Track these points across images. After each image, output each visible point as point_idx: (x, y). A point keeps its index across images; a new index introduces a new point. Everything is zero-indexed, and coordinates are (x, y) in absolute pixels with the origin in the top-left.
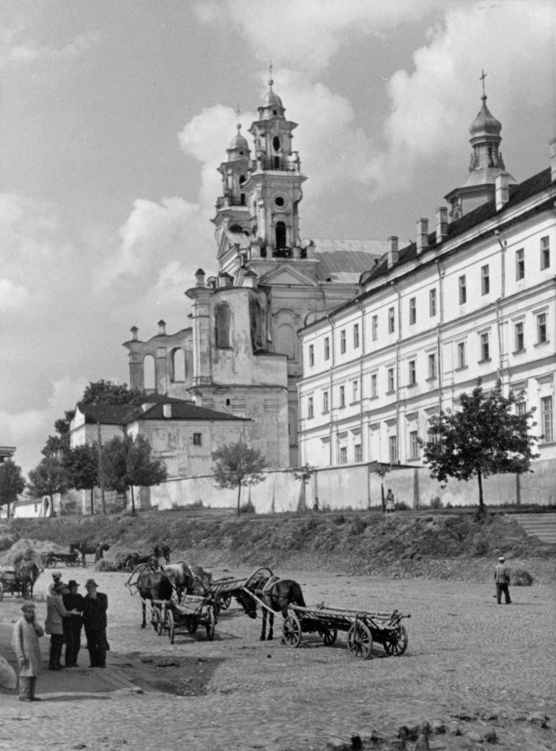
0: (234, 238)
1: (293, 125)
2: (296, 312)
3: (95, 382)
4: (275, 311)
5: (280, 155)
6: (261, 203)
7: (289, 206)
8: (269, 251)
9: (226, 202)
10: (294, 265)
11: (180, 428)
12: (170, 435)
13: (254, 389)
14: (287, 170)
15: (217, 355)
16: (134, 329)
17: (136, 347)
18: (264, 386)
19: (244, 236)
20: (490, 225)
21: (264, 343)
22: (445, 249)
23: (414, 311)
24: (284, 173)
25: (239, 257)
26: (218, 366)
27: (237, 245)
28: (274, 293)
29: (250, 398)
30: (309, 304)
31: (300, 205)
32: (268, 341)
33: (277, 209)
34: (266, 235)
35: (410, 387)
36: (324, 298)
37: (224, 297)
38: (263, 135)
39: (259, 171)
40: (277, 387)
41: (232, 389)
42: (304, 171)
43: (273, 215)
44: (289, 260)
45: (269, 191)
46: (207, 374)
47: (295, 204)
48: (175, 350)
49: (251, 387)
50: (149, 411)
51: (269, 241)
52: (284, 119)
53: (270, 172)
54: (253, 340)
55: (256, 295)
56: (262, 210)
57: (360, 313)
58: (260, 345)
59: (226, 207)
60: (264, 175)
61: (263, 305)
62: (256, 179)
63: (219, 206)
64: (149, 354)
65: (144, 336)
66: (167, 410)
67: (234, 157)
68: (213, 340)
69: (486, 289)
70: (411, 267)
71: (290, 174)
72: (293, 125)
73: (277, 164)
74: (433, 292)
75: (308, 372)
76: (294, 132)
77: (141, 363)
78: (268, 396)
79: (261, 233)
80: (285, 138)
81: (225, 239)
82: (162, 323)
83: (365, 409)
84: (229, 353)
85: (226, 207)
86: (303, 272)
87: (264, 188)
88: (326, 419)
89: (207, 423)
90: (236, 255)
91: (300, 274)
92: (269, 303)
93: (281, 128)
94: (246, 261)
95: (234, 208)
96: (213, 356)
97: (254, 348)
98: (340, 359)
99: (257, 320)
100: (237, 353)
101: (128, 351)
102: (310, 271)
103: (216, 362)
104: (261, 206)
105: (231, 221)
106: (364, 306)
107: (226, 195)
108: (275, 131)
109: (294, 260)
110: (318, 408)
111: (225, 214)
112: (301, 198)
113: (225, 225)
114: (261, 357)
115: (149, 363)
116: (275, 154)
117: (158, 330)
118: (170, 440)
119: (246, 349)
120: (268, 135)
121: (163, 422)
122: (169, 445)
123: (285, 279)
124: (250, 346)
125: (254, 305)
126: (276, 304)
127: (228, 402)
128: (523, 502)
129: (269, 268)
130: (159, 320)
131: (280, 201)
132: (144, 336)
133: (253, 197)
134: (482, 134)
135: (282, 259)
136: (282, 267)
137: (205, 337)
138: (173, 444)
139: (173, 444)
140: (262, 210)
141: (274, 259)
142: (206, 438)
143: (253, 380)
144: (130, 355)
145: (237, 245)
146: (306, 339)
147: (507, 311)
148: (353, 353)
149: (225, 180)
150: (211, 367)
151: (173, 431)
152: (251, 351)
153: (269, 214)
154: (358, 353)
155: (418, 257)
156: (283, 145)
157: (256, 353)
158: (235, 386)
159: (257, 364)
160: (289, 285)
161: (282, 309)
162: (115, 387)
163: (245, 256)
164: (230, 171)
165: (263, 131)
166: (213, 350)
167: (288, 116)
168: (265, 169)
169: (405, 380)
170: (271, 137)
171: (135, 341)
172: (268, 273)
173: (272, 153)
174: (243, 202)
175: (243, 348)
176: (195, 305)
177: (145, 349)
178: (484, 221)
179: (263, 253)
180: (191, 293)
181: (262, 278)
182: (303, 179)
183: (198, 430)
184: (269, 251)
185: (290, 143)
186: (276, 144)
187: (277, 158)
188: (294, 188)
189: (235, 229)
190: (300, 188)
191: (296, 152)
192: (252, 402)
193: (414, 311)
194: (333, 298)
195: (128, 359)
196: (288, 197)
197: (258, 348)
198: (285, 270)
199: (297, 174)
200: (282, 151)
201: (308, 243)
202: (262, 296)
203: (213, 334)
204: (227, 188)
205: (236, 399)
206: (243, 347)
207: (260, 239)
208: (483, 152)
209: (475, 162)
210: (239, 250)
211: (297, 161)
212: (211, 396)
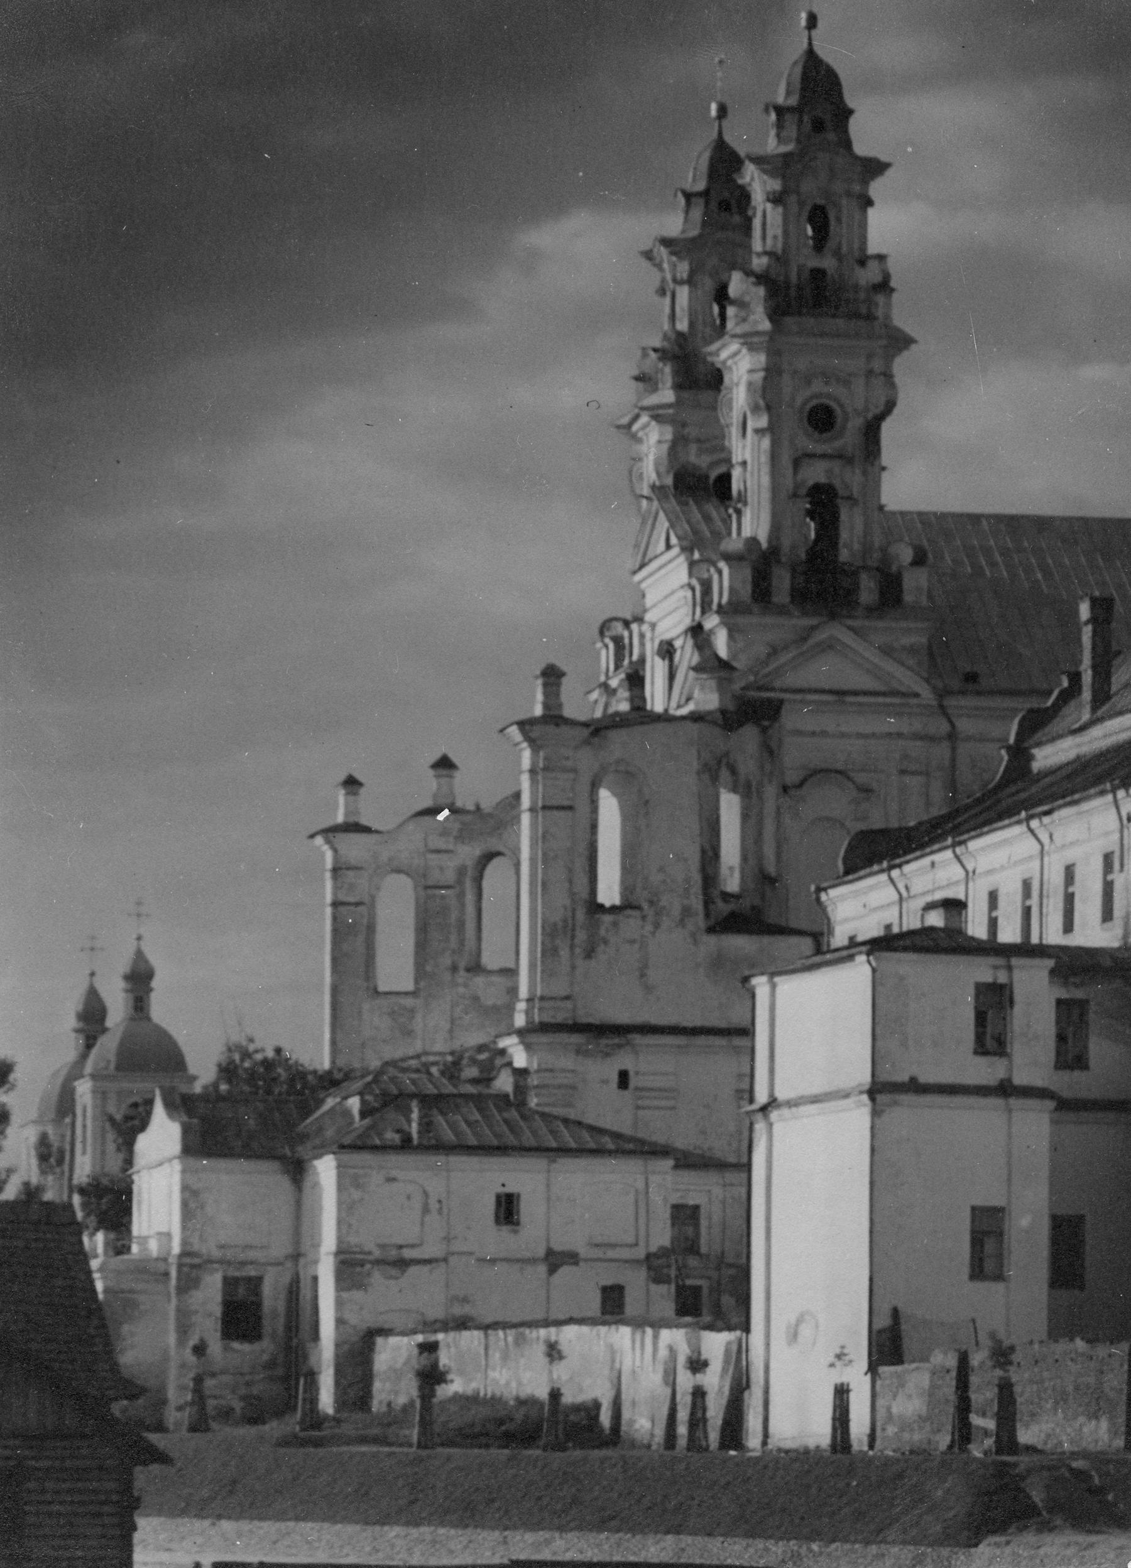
1: (875, 168)
2: (861, 778)
4: (792, 777)
5: (828, 263)
7: (850, 437)
13: (701, 1040)
17: (355, 847)
23: (1069, 899)
26: (593, 963)
28: (790, 720)
30: (905, 757)
31: (888, 429)
36: (952, 736)
38: (776, 199)
41: (637, 1039)
43: (797, 463)
45: (787, 383)
46: (560, 988)
48: (489, 857)
51: (786, 543)
52: (847, 144)
64: (399, 871)
72: (875, 168)
76: (876, 188)
77: (369, 904)
82: (444, 764)
85: (666, 395)
87: (772, 372)
91: (876, 659)
100: (657, 925)
102: (912, 650)
103: (589, 954)
107: (663, 354)
112: (890, 406)
116: (814, 263)
119: (686, 912)
120: (793, 199)
124: (697, 904)
127: (624, 1079)
130: (435, 756)
136: (821, 636)
142: (530, 1210)
150: (573, 967)
152: (701, 921)
153: (786, 460)
159: (718, 963)
161: (816, 772)
165: (776, 185)
166: (581, 915)
170: (801, 204)
171: (353, 827)
175: (676, 911)
184: (782, 582)
185: (863, 225)
187: (818, 274)
188: (870, 373)
190: (888, 376)
191: (881, 258)
197: (722, 908)
198: (829, 646)
200: (838, 254)
202: (749, 735)
206: (673, 903)
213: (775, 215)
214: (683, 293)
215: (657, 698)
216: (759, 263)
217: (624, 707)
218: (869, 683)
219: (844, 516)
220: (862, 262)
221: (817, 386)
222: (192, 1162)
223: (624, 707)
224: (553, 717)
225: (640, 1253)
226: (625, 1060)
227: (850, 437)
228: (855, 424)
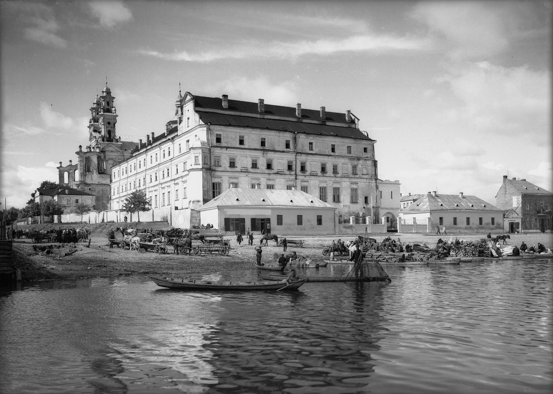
0: (94, 134)
1: (114, 98)
2: (114, 160)
3: (44, 181)
4: (107, 159)
5: (109, 108)
6: (103, 123)
7: (112, 125)
8: (105, 139)
9: (93, 122)
10: (113, 144)
11: (71, 198)
12: (68, 200)
14: (112, 113)
15: (86, 174)
16: (61, 163)
18: (102, 184)
19: (98, 133)
20: (164, 140)
21: (103, 170)
22: (148, 148)
23: (140, 164)
24: (110, 114)
25: (95, 141)
27: (95, 137)
28: (107, 153)
29: (97, 188)
32: (104, 169)
33: (108, 125)
34: (104, 134)
35: (139, 187)
36: (124, 156)
37: (88, 155)
39: (102, 113)
40: (107, 184)
42: (117, 113)
43: (107, 128)
44: (112, 143)
47: (114, 125)
49: (97, 184)
50: (61, 192)
53: (105, 113)
54: (98, 169)
55: (100, 155)
56: (103, 126)
57: (127, 164)
58: (101, 171)
59: (92, 123)
60: (103, 114)
61: (102, 158)
62: (101, 115)
63: (90, 122)
65: (64, 165)
66: (67, 191)
67: (95, 106)
68: (85, 169)
69: (157, 161)
70: (145, 149)
71: (112, 114)
72: (114, 98)
73: (109, 111)
74: (145, 159)
75: (114, 180)
78: (103, 188)
79: (103, 133)
80: (111, 102)
81: (91, 134)
82: (71, 161)
83: (128, 193)
84: (90, 173)
86: (116, 147)
88: (118, 196)
89: (80, 196)
90: (95, 140)
92: (105, 157)
93: (109, 99)
94: (98, 143)
95: (95, 123)
96: (85, 174)
97: (99, 172)
98: (122, 177)
99: (100, 163)
101: (58, 170)
102: (119, 147)
104: (103, 124)
105: (94, 127)
106: (128, 162)
107: (93, 119)
108: (107, 100)
109: (114, 143)
110: (116, 193)
111: (92, 125)
113: (92, 129)
114: (101, 175)
115: (66, 175)
117: (69, 163)
118: (68, 201)
119: (96, 172)
121: (65, 195)
122: (67, 203)
123: (111, 149)
125: (99, 158)
126: (107, 157)
128: (155, 220)
129: (105, 145)
131: (109, 123)
132: (64, 165)
133: (100, 121)
134: (179, 103)
135: (110, 142)
136: (110, 145)
137: (82, 168)
138: (69, 203)
139: (69, 203)
140: (103, 126)
141: (107, 142)
142: (80, 201)
143: (98, 182)
144: (59, 171)
145: (95, 137)
146: (113, 170)
147: (161, 167)
148: (125, 176)
149: (92, 113)
151: (69, 199)
153: (105, 127)
154: (135, 172)
155: (146, 147)
156: (110, 105)
157: (99, 173)
158: (92, 184)
160: (112, 151)
162: (51, 183)
163: (97, 140)
164: (94, 111)
167: (112, 95)
168: (104, 112)
169: (138, 185)
171: (61, 166)
172: (105, 147)
173: (107, 107)
174: (97, 122)
176: (79, 157)
177: (65, 169)
178: (162, 138)
179: (103, 140)
180: (77, 153)
181: (103, 148)
182: (117, 116)
183: (77, 198)
186: (108, 104)
187: (108, 109)
189: (95, 131)
191: (115, 107)
192: (98, 189)
193: (140, 164)
194: (127, 156)
195: (58, 173)
196: (112, 122)
197: (100, 172)
198: (110, 146)
199: (115, 114)
200: (110, 107)
201: (118, 138)
202: (102, 155)
203: (84, 167)
204: (93, 117)
205: (93, 188)
207: (102, 135)
208: (179, 109)
209: (177, 113)
210: (96, 138)
211: (115, 110)
212: (84, 187)
213: (103, 102)
214: (94, 113)
215: (92, 150)
216: (102, 107)
217: (89, 151)
218: (115, 150)
219: (112, 133)
220: (113, 108)
221: (109, 121)
222: (41, 196)
223: (89, 151)
224: (81, 151)
225: (92, 206)
226: (89, 187)
227: (112, 125)
228: (113, 124)
